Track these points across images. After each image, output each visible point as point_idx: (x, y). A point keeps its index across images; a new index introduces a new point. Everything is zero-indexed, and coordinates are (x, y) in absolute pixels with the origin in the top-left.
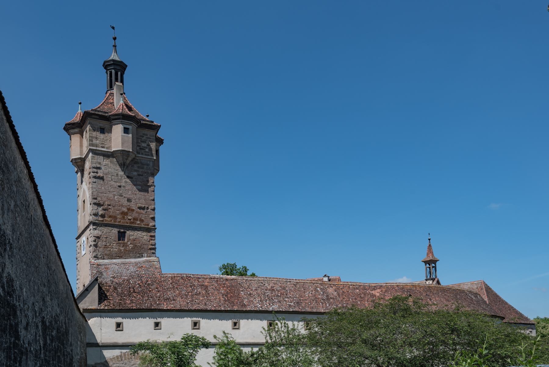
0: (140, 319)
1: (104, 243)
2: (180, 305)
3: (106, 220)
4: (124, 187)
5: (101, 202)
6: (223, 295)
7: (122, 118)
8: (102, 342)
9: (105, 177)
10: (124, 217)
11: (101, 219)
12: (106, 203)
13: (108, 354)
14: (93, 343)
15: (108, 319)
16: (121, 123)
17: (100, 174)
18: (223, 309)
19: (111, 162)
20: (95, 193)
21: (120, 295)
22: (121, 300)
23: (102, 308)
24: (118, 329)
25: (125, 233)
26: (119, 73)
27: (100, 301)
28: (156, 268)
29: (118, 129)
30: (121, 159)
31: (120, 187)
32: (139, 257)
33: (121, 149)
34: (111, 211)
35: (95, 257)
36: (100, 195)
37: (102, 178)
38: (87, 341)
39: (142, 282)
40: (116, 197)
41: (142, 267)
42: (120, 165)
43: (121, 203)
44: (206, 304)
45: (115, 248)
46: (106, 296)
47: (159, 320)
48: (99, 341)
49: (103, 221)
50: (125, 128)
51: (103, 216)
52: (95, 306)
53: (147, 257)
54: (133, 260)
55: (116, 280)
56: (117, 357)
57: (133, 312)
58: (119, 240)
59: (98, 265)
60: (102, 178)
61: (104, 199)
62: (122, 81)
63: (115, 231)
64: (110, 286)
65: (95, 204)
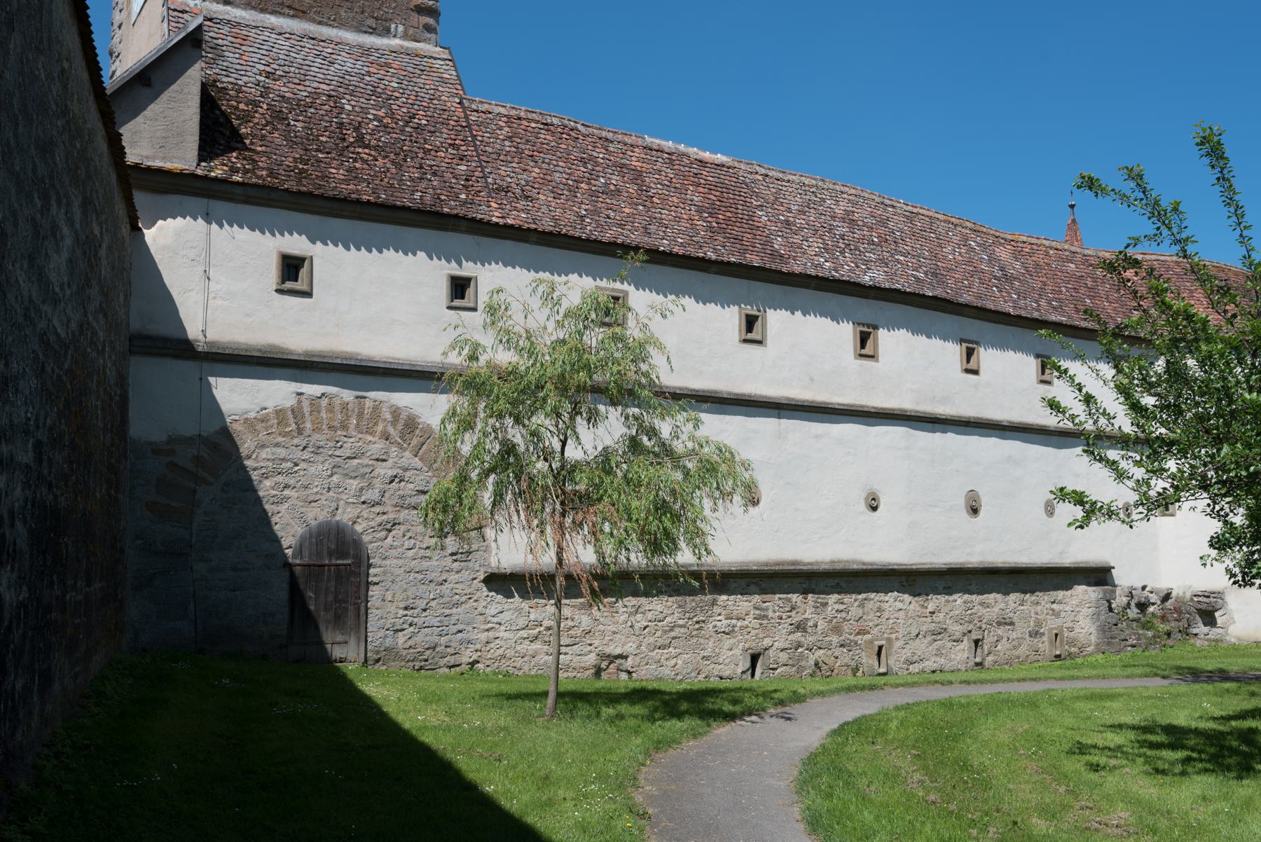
0: (390, 254)
2: (553, 218)
6: (700, 211)
8: (211, 336)
13: (236, 397)
14: (166, 340)
15: (244, 235)
18: (711, 255)
23: (217, 173)
24: (289, 285)
27: (208, 150)
28: (444, 81)
32: (373, 31)
38: (135, 325)
39: (391, 114)
44: (646, 232)
47: (468, 269)
48: (193, 330)
53: (405, 36)
56: (279, 413)
57: (361, 218)
64: (256, 104)
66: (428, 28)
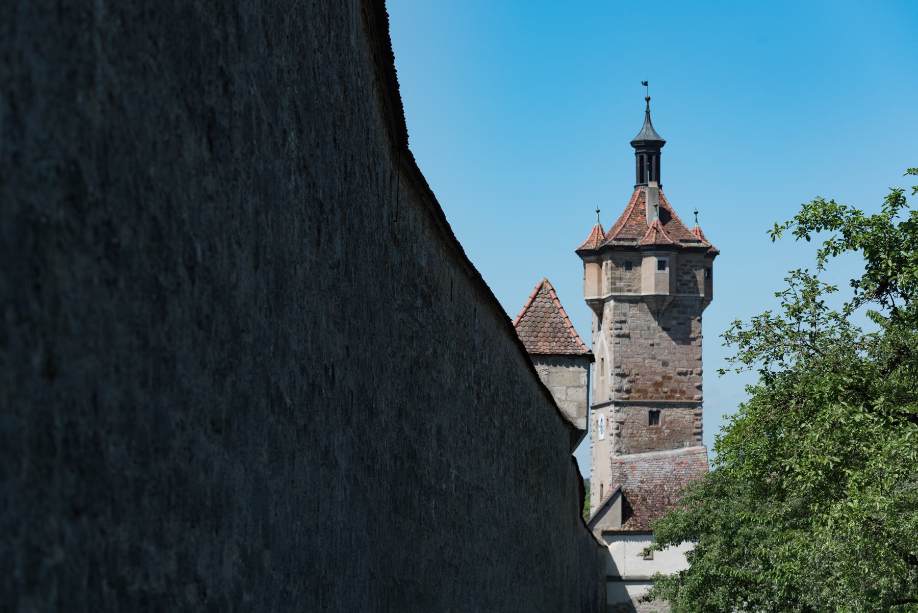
1: (630, 431)
3: (633, 397)
4: (658, 344)
5: (627, 372)
7: (656, 249)
9: (632, 335)
10: (657, 390)
11: (627, 396)
12: (634, 372)
13: (635, 592)
16: (655, 256)
17: (625, 331)
19: (640, 310)
20: (618, 359)
21: (650, 508)
22: (651, 516)
25: (658, 412)
26: (654, 157)
27: (625, 518)
28: (702, 464)
29: (650, 264)
30: (654, 305)
31: (652, 345)
32: (678, 447)
33: (653, 293)
34: (640, 384)
35: (617, 451)
36: (625, 360)
37: (627, 336)
38: (607, 573)
40: (646, 361)
41: (682, 463)
42: (653, 313)
43: (653, 370)
45: (645, 436)
46: (632, 511)
48: (621, 573)
49: (628, 398)
50: (659, 262)
51: (628, 391)
52: (617, 526)
53: (690, 446)
54: (669, 453)
55: (645, 486)
58: (650, 424)
59: (622, 463)
60: (627, 336)
61: (631, 366)
62: (658, 180)
63: (645, 411)
65: (618, 375)
66: (698, 440)
